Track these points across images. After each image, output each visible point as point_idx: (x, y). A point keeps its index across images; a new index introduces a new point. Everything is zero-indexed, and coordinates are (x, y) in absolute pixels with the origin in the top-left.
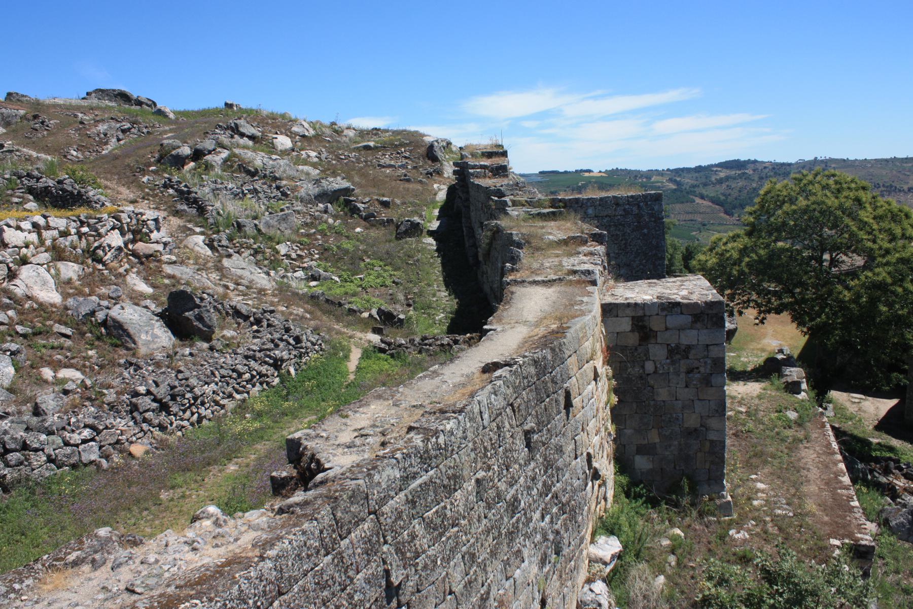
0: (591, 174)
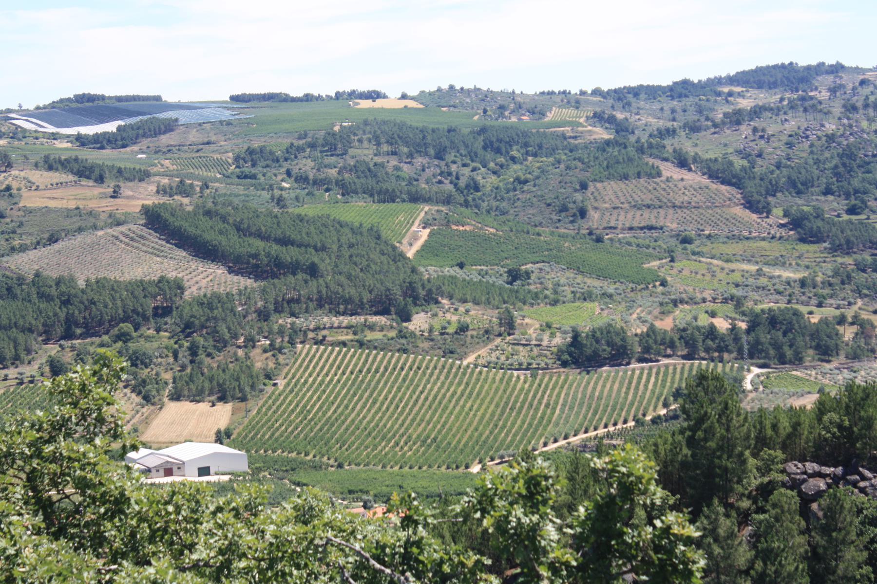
0: (379, 103)
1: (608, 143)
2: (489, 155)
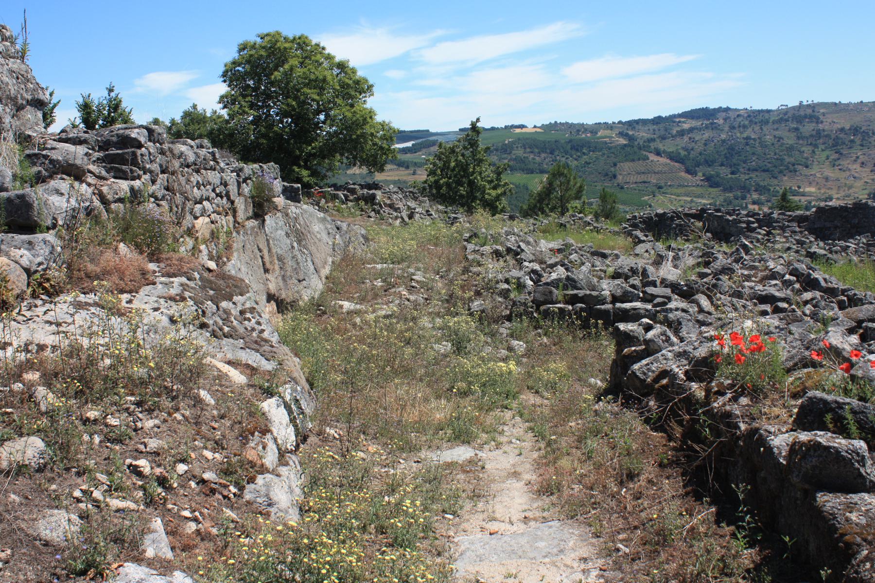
0: (524, 130)
1: (625, 145)
2: (573, 152)
